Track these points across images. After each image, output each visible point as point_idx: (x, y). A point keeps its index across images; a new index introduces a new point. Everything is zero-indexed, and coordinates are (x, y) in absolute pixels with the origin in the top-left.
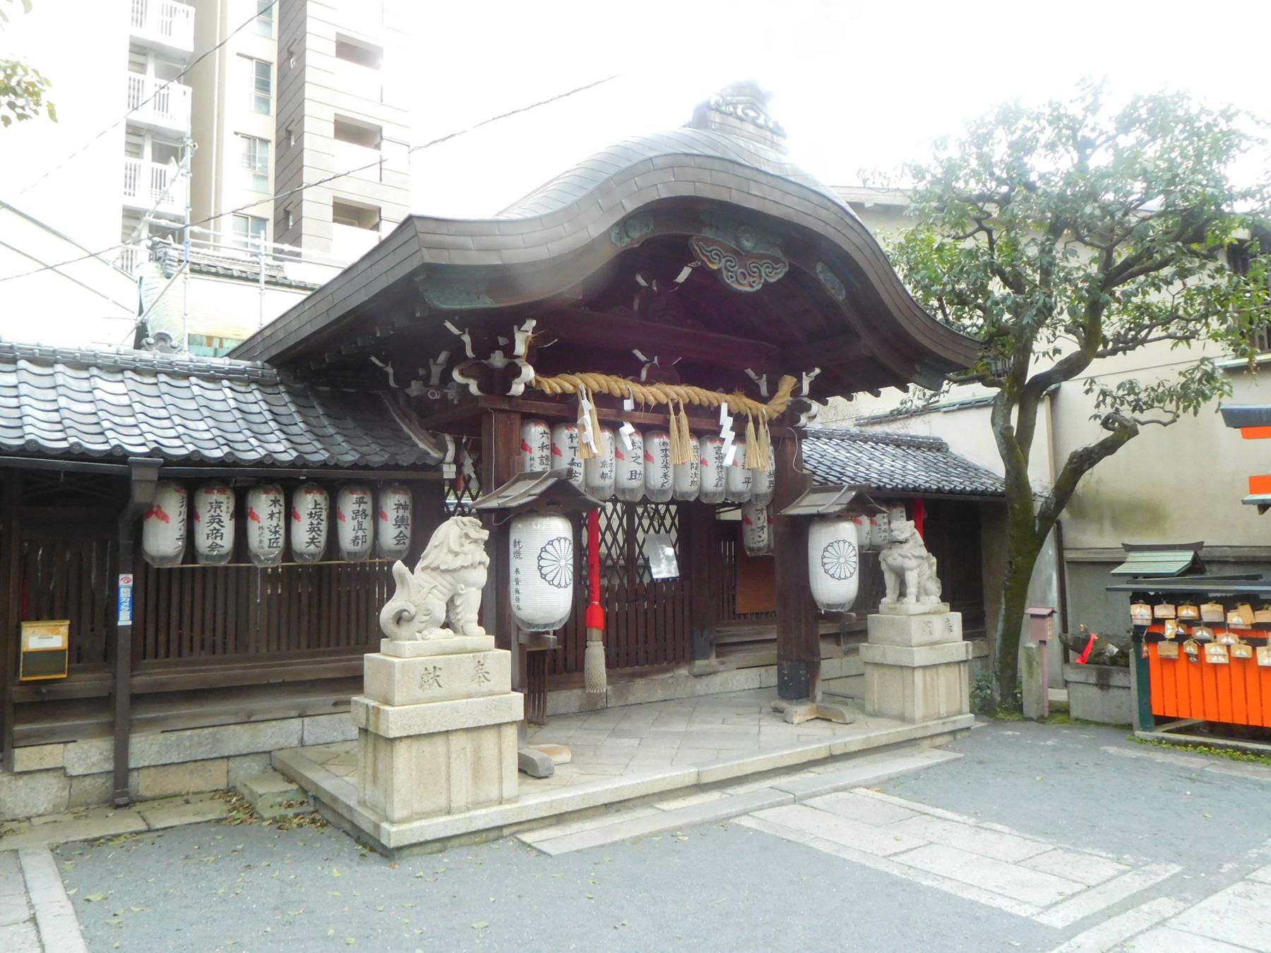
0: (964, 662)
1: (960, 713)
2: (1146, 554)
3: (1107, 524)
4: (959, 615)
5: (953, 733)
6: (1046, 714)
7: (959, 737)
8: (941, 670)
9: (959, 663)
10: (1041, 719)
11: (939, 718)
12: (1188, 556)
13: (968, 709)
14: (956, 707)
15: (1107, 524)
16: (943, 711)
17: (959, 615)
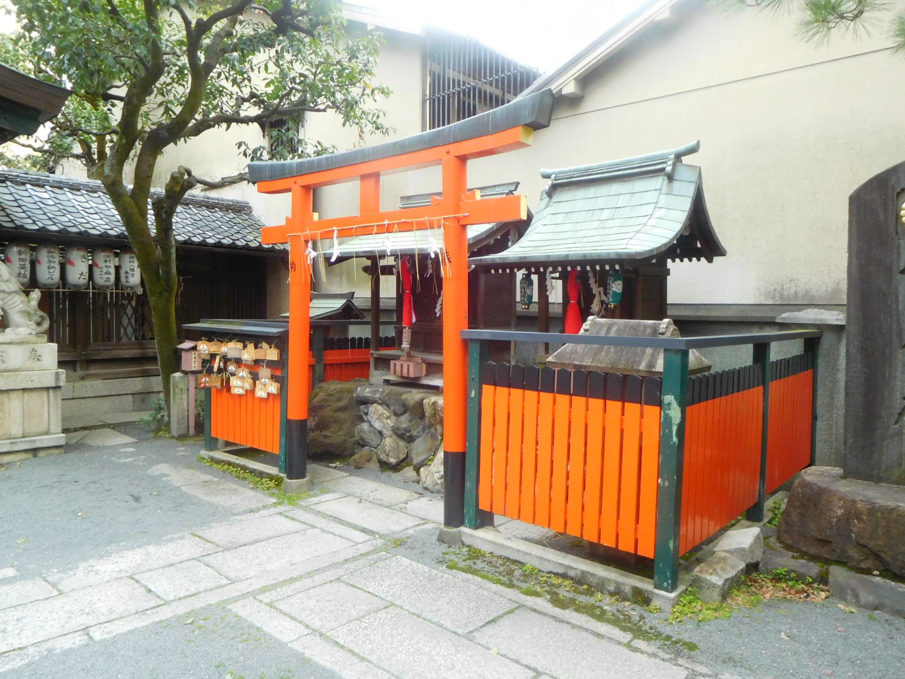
0: (57, 388)
1: (47, 433)
2: (322, 301)
3: (344, 279)
4: (54, 346)
5: (35, 451)
6: (192, 431)
7: (42, 454)
8: (14, 396)
9: (47, 389)
10: (182, 437)
11: (8, 439)
12: (338, 304)
13: (60, 429)
14: (43, 427)
15: (344, 279)
16: (16, 430)
17: (54, 346)
